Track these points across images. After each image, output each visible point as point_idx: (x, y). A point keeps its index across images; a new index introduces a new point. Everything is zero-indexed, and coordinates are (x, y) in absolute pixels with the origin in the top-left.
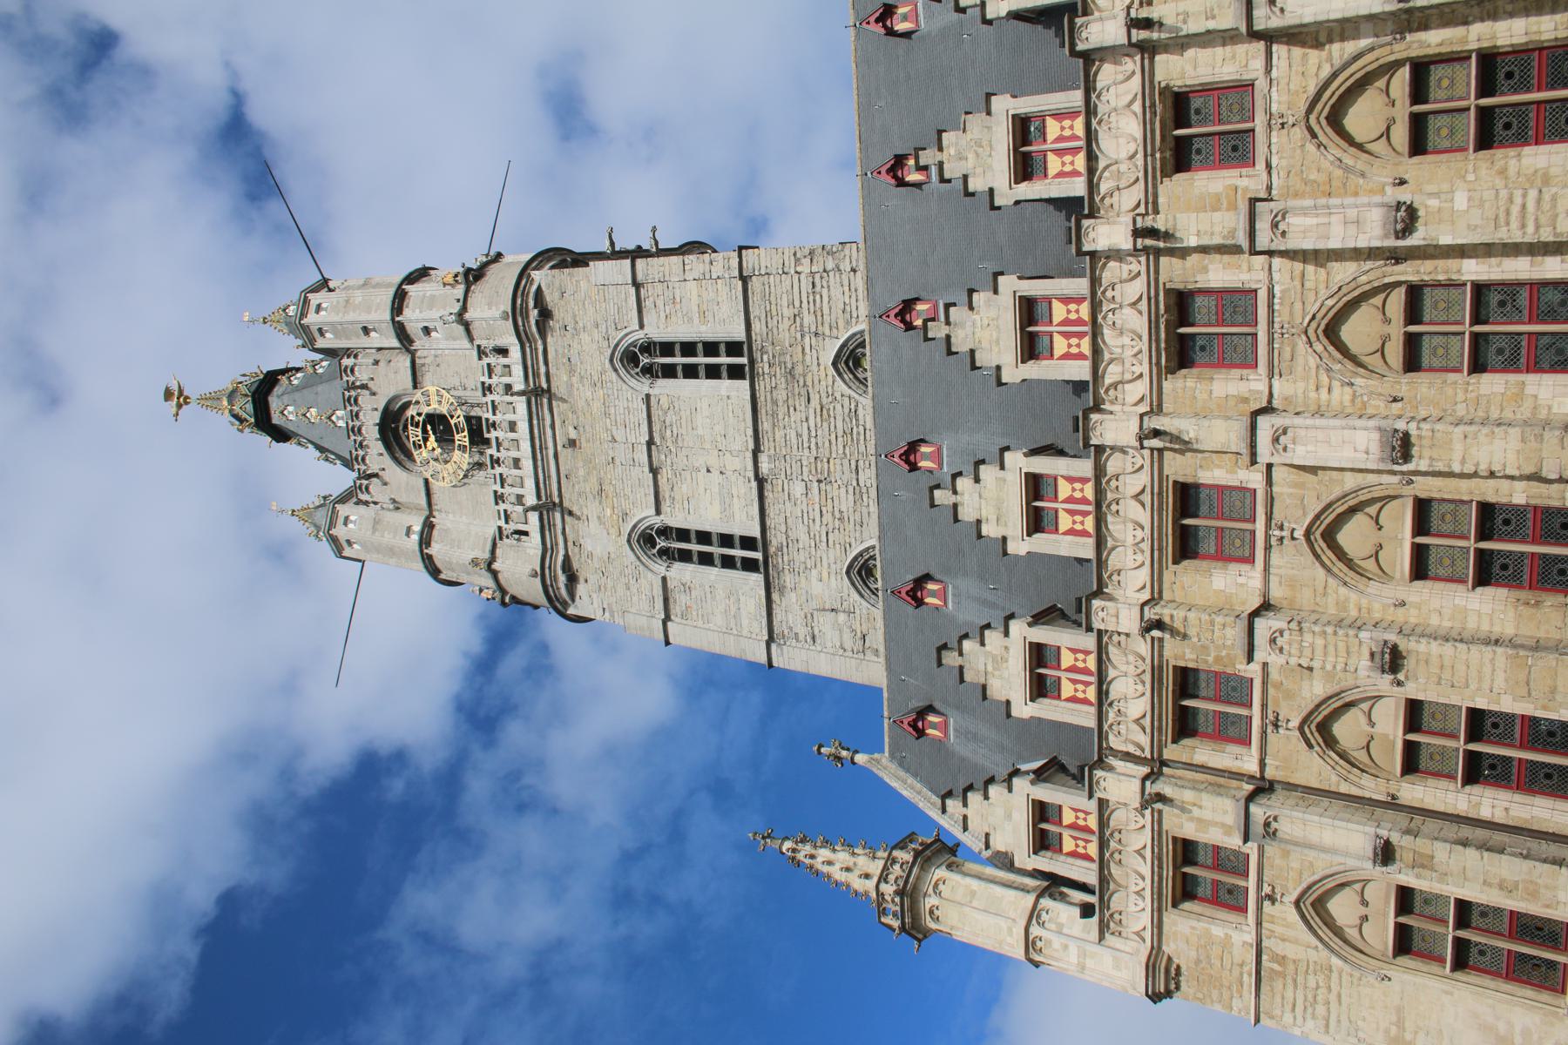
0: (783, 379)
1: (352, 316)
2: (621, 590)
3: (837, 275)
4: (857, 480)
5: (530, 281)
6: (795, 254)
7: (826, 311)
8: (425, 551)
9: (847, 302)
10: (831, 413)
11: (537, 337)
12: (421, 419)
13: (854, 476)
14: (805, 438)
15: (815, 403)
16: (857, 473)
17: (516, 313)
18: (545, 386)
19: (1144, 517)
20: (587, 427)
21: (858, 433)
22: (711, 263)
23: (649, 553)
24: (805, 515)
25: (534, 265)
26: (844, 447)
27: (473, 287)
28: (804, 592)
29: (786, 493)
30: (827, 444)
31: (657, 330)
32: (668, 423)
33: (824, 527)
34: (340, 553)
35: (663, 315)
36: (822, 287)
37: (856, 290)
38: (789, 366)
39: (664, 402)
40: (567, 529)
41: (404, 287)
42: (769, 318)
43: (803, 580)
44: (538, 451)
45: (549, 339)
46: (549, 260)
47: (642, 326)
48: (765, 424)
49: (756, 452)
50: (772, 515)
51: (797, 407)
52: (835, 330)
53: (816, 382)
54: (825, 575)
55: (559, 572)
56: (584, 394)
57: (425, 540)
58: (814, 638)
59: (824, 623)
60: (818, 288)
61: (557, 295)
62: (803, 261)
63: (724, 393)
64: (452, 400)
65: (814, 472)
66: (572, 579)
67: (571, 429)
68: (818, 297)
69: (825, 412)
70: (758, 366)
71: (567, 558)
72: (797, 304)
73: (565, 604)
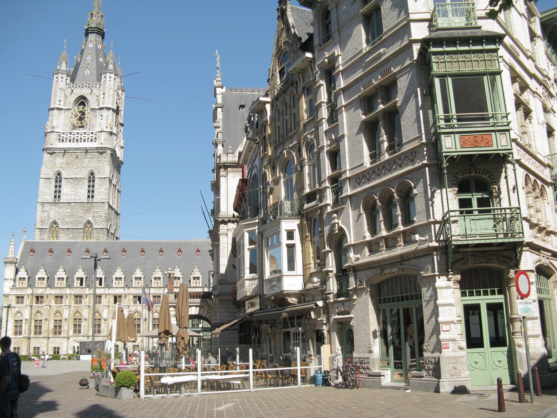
1: (107, 90)
2: (49, 166)
5: (108, 150)
15: (83, 215)
17: (102, 148)
19: (59, 293)
31: (96, 180)
39: (84, 181)
46: (113, 151)
49: (75, 203)
56: (86, 161)
57: (58, 109)
59: (46, 214)
61: (105, 156)
66: (51, 154)
70: (89, 204)
71: (55, 153)
73: (46, 151)
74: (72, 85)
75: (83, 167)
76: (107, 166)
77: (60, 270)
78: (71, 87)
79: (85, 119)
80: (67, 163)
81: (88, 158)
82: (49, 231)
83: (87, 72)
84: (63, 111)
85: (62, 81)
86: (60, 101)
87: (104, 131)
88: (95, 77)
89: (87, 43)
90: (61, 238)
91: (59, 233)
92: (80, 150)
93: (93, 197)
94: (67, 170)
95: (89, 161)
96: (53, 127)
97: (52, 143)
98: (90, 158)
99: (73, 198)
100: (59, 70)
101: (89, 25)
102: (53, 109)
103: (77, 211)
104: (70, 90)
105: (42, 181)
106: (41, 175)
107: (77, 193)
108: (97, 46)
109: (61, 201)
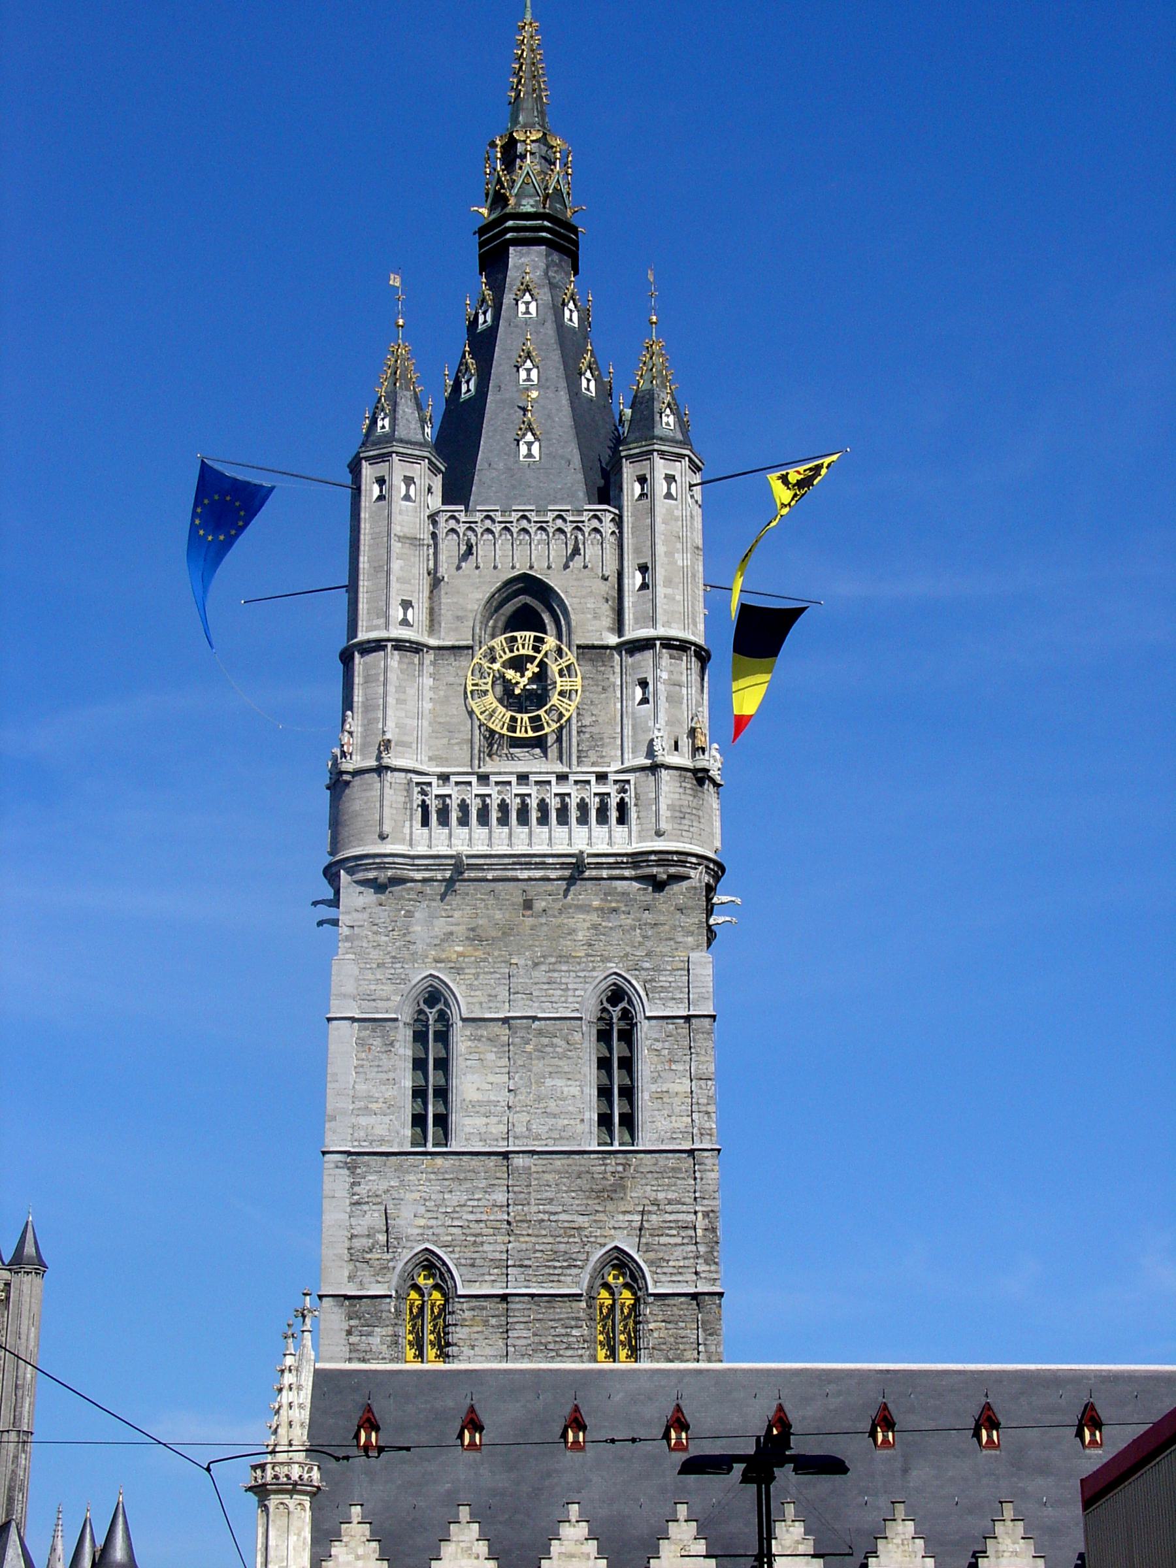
0: (600, 1187)
1: (660, 549)
3: (691, 1255)
4: (514, 1266)
6: (712, 1211)
7: (663, 1240)
8: (389, 644)
9: (671, 1263)
10: (571, 1240)
11: (640, 872)
13: (517, 1263)
14: (548, 1208)
15: (581, 1221)
16: (521, 1266)
17: (664, 858)
18: (587, 874)
20: (545, 928)
21: (555, 1268)
22: (707, 1113)
23: (419, 997)
24: (476, 1203)
25: (711, 866)
27: (689, 774)
28: (402, 1196)
29: (493, 1183)
30: (544, 1232)
31: (645, 1032)
32: (555, 1040)
33: (467, 1224)
34: (367, 459)
35: (658, 1046)
36: (683, 1238)
37: (680, 1273)
38: (613, 1195)
39: (577, 1037)
41: (693, 648)
42: (656, 1175)
43: (410, 1196)
45: (636, 885)
47: (649, 1018)
48: (558, 1163)
49: (533, 1153)
50: (473, 1163)
51: (577, 1202)
52: (643, 1248)
53: (601, 1224)
55: (390, 873)
56: (582, 923)
57: (400, 645)
58: (357, 1203)
63: (587, 1116)
64: (567, 715)
65: (518, 1218)
67: (544, 904)
68: (674, 1232)
72: (669, 1208)
73: (350, 871)
74: (462, 517)
75: (563, 958)
76: (694, 956)
77: (566, 1531)
78: (461, 529)
79: (555, 699)
80: (475, 937)
81: (585, 908)
82: (398, 1313)
83: (530, 449)
84: (429, 657)
85: (407, 498)
86: (406, 605)
87: (668, 767)
88: (574, 478)
89: (508, 299)
90: (467, 1351)
91: (450, 1319)
92: (543, 866)
93: (628, 1121)
94: (477, 976)
95: (595, 927)
96: (387, 744)
97: (387, 829)
98: (597, 909)
99: (520, 1129)
100: (389, 438)
101: (499, 200)
102: (377, 646)
104: (449, 548)
105: (343, 1037)
106: (334, 1002)
107: (539, 1099)
108: (559, 315)
109: (454, 1146)
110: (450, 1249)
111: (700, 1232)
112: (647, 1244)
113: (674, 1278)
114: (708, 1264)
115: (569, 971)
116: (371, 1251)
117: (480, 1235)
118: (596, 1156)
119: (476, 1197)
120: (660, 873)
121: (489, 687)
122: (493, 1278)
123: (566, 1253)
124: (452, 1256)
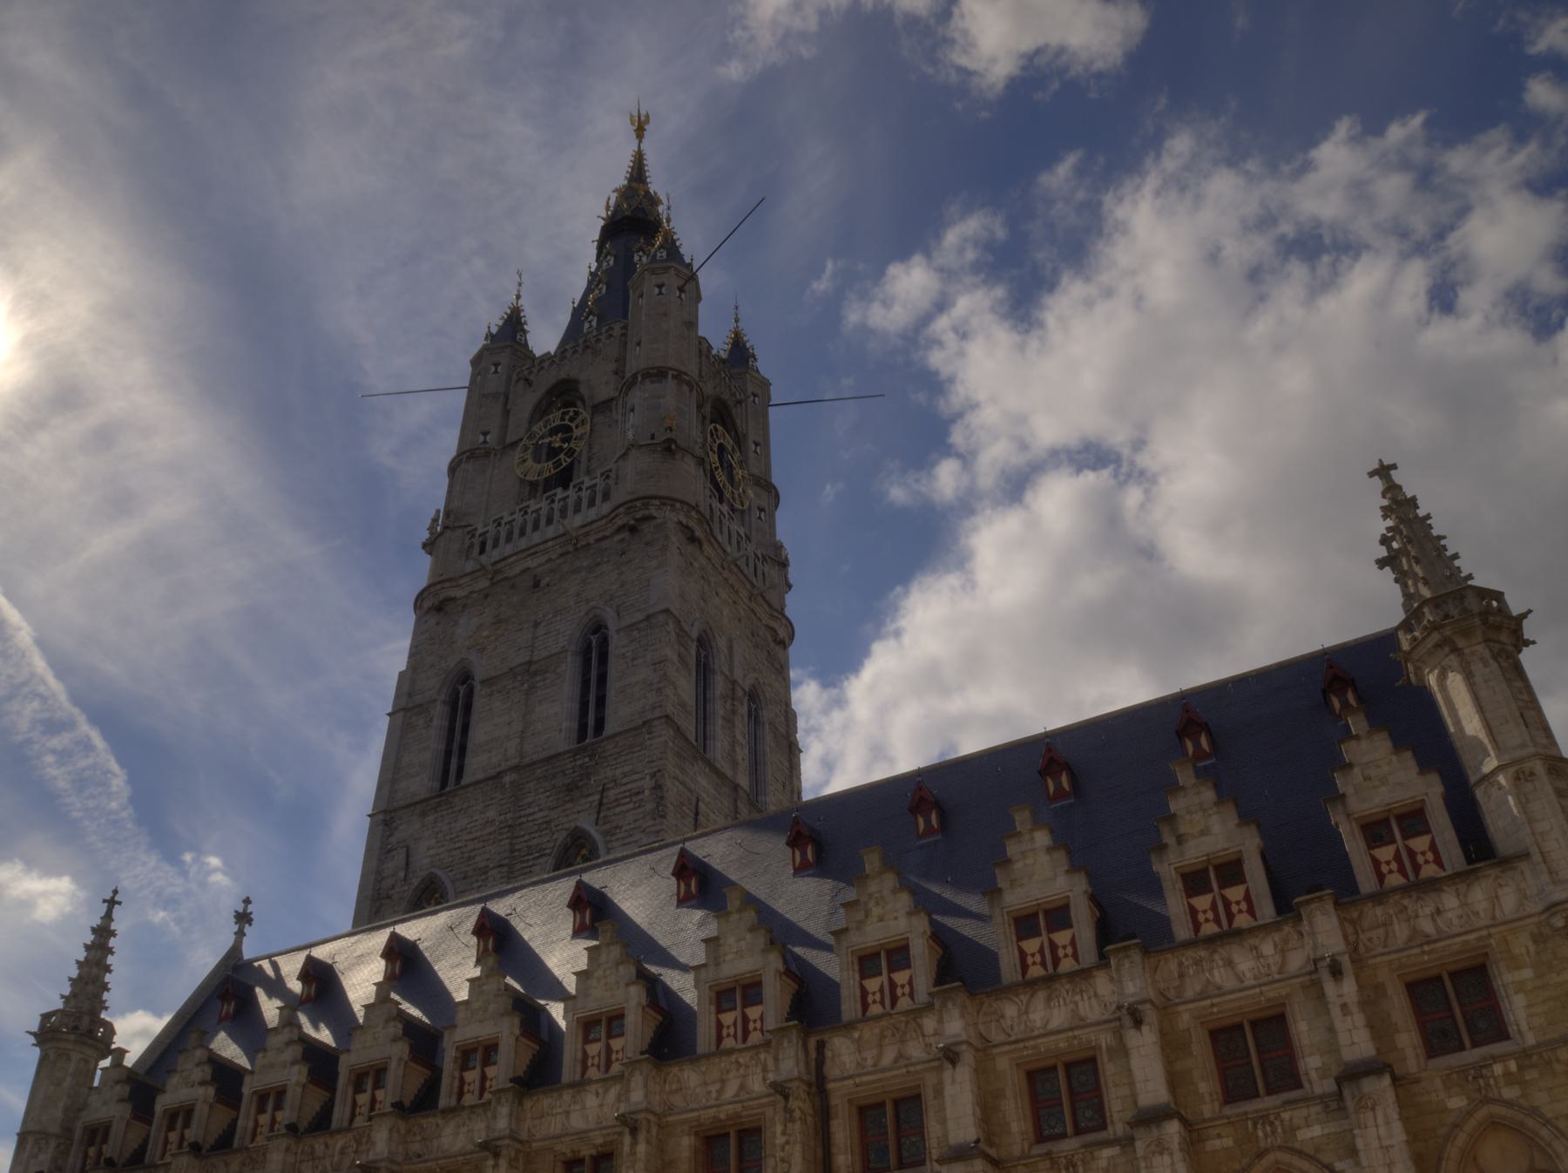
4: (494, 868)
7: (618, 810)
9: (623, 829)
11: (615, 527)
12: (567, 422)
14: (528, 811)
18: (579, 545)
21: (528, 861)
26: (519, 850)
29: (490, 802)
30: (522, 833)
36: (635, 802)
37: (631, 836)
40: (475, 595)
44: (528, 552)
45: (617, 538)
48: (539, 771)
51: (551, 799)
54: (432, 852)
60: (634, 799)
62: (653, 782)
67: (547, 579)
68: (628, 800)
69: (545, 826)
72: (624, 781)
86: (485, 434)
103: (530, 805)
110: (450, 869)
111: (647, 792)
112: (605, 817)
113: (626, 841)
114: (655, 819)
115: (561, 620)
116: (393, 887)
117: (474, 850)
118: (568, 755)
119: (474, 819)
120: (628, 521)
121: (529, 456)
122: (479, 884)
123: (538, 845)
124: (450, 874)
